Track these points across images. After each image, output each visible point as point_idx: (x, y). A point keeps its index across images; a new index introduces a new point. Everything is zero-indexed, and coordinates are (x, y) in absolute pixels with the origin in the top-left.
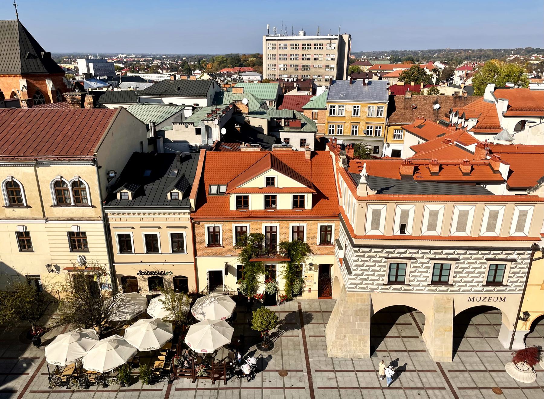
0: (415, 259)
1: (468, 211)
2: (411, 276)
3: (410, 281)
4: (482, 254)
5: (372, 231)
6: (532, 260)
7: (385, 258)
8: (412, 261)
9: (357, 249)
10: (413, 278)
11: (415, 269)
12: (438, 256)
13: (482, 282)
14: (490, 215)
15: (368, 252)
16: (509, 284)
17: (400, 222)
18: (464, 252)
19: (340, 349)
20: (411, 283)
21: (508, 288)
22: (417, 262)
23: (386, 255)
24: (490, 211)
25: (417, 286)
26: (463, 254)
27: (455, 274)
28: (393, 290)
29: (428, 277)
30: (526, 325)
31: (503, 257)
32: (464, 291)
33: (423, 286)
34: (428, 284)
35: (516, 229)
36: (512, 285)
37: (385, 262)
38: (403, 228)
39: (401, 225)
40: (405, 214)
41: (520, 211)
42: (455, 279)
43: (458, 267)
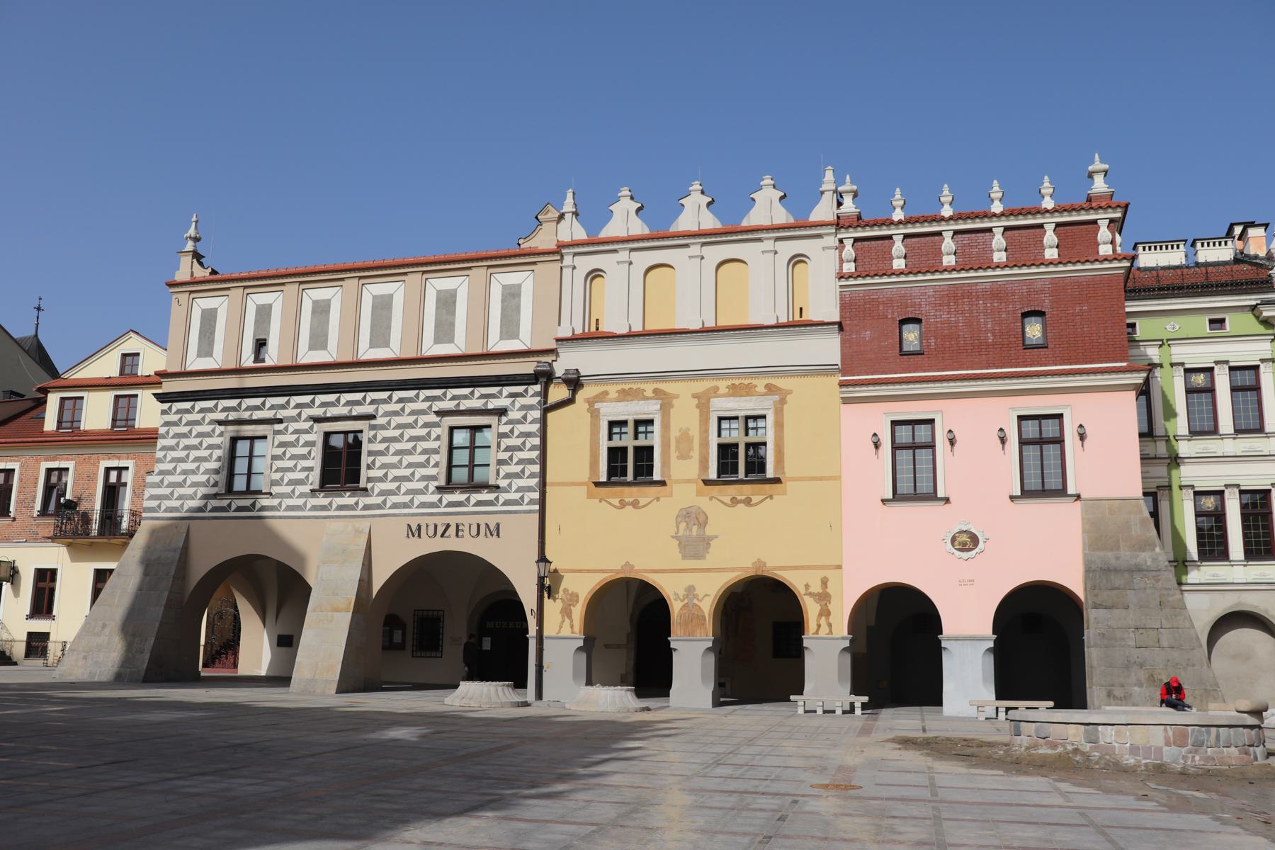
0: (280, 421)
1: (391, 296)
2: (274, 468)
3: (274, 483)
4: (427, 399)
5: (198, 359)
6: (547, 409)
7: (220, 423)
8: (278, 427)
9: (166, 406)
10: (277, 476)
11: (283, 449)
12: (332, 412)
13: (434, 478)
14: (438, 300)
15: (187, 411)
16: (503, 483)
17: (254, 337)
18: (384, 395)
19: (85, 658)
20: (275, 490)
21: (504, 497)
22: (286, 429)
23: (222, 416)
24: (438, 292)
25: (289, 496)
26: (384, 401)
27: (371, 459)
28: (237, 510)
29: (310, 469)
30: (570, 617)
31: (476, 404)
32: (395, 506)
33: (302, 495)
34: (312, 491)
35: (501, 332)
36: (510, 485)
37: (221, 434)
38: (260, 344)
39: (258, 340)
40: (264, 313)
41: (504, 287)
42: (372, 473)
43: (375, 437)
